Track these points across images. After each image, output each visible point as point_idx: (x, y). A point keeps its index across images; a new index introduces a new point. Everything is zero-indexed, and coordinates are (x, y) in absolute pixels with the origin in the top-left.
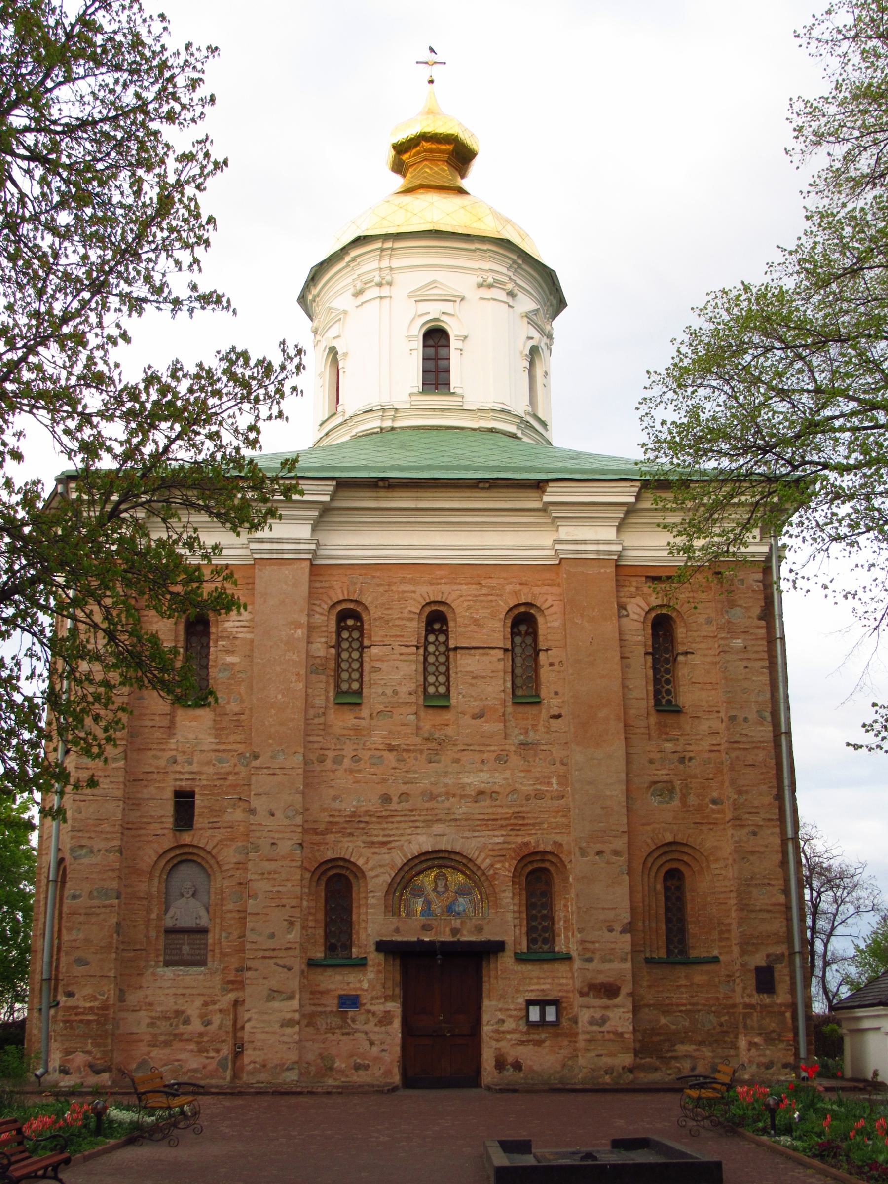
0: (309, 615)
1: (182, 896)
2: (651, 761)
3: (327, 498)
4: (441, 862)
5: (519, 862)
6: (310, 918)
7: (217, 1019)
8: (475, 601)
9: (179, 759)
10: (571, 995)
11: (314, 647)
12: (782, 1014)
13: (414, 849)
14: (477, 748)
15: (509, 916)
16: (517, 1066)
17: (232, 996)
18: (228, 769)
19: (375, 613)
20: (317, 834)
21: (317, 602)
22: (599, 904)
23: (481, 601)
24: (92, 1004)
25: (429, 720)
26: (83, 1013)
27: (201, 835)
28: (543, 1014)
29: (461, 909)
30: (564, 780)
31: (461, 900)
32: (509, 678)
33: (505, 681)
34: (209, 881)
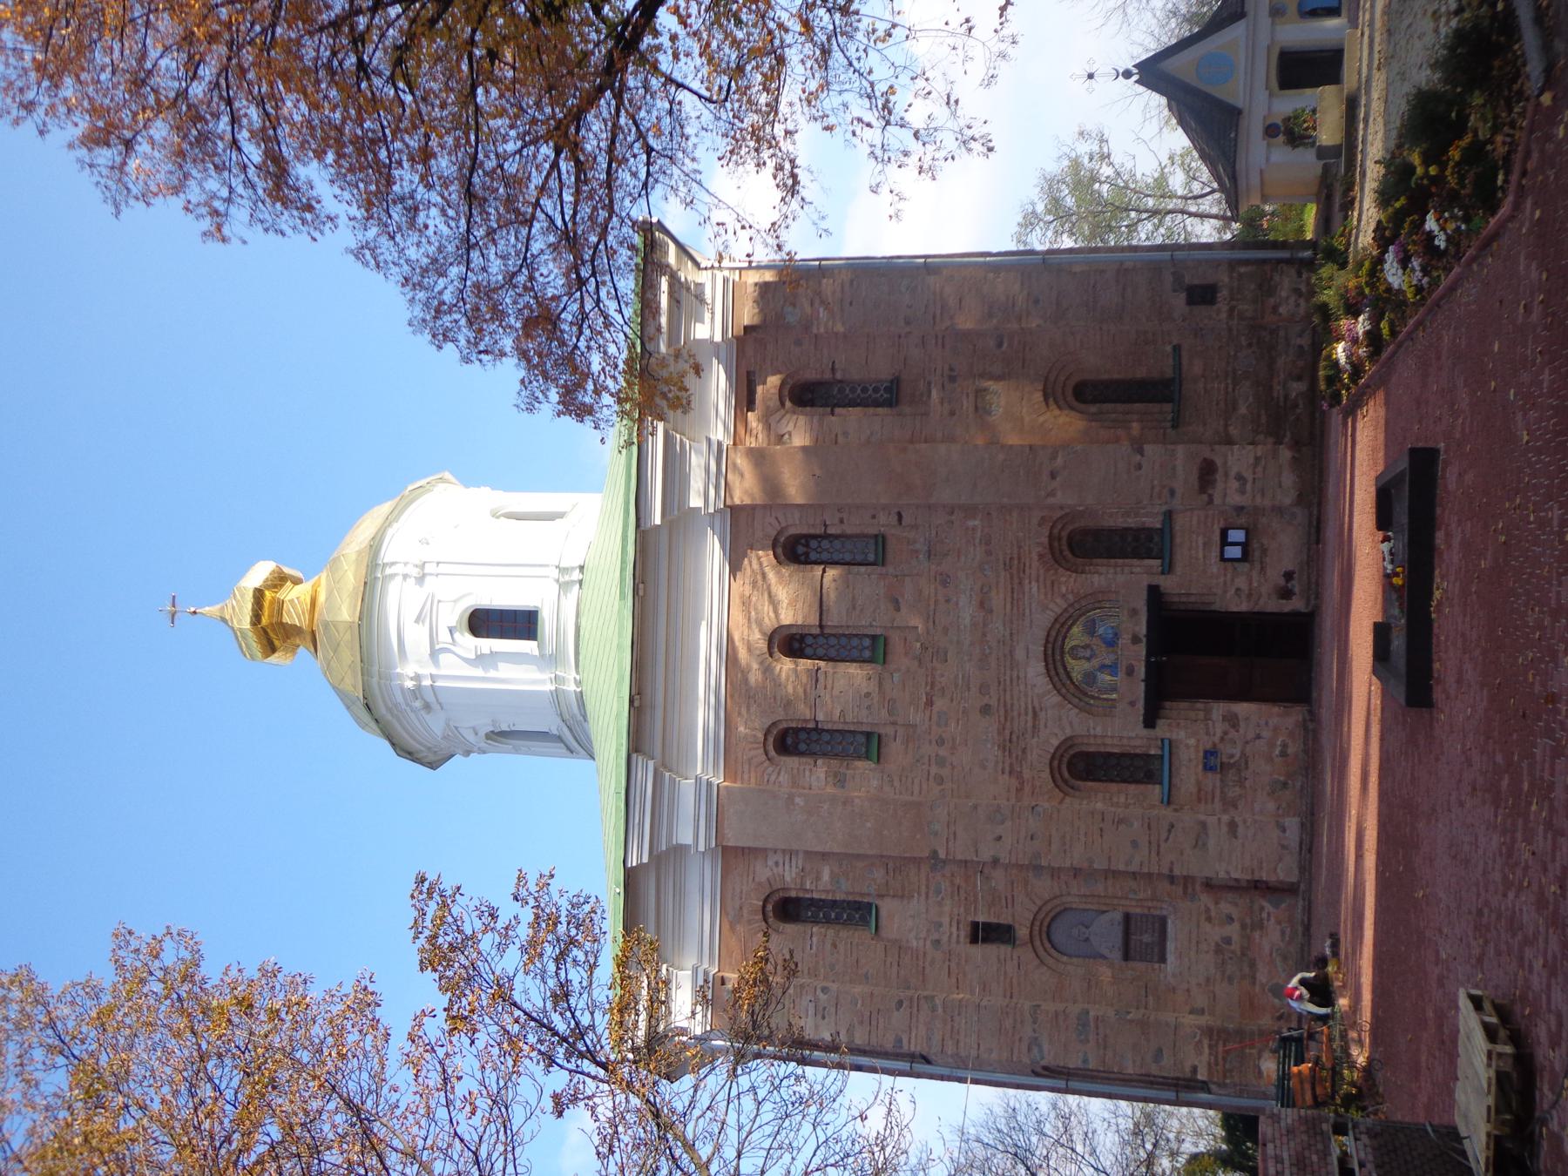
1: (1087, 940)
2: (952, 413)
3: (651, 764)
4: (1058, 652)
9: (936, 936)
12: (1241, 275)
15: (1121, 578)
16: (1289, 576)
19: (780, 714)
25: (900, 660)
27: (1020, 917)
30: (970, 511)
31: (1101, 631)
32: (856, 569)
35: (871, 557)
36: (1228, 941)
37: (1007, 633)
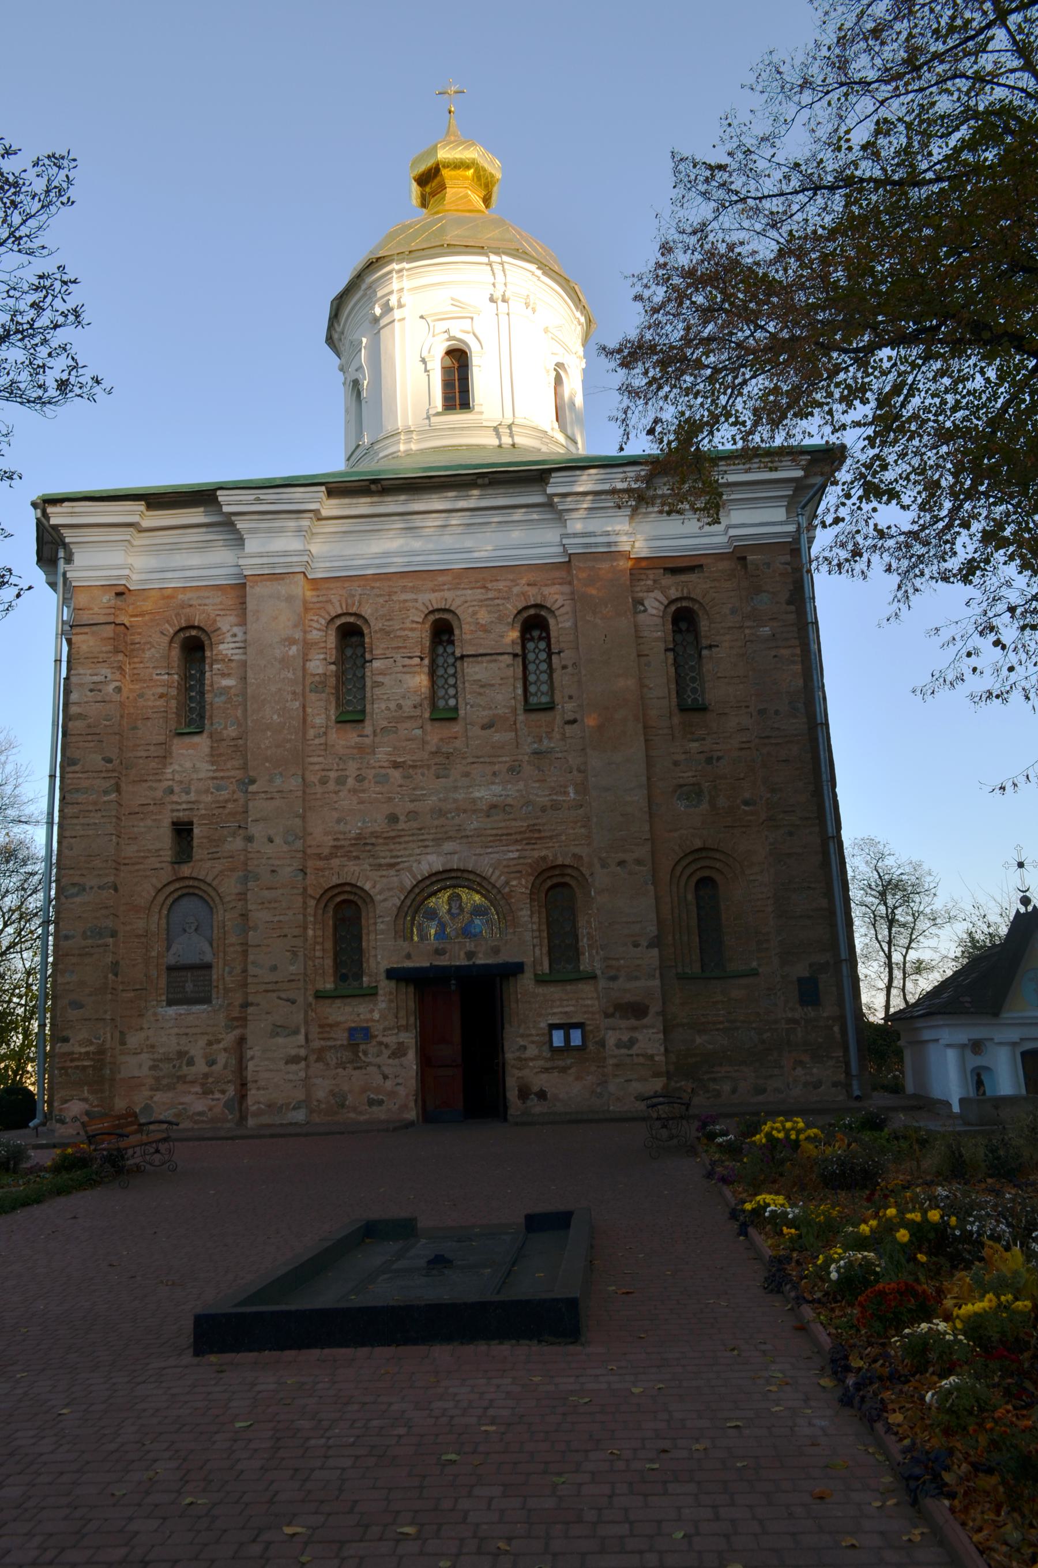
2: (676, 763)
5: (537, 877)
6: (318, 947)
7: (222, 1059)
9: (177, 789)
10: (597, 1016)
14: (487, 760)
15: (528, 936)
16: (542, 1095)
17: (237, 1032)
18: (227, 796)
19: (376, 625)
20: (321, 859)
21: (315, 618)
23: (487, 606)
24: (88, 1049)
25: (435, 735)
26: (78, 1059)
27: (202, 866)
28: (567, 1038)
30: (582, 788)
31: (477, 922)
32: (519, 685)
33: (515, 688)
35: (533, 700)
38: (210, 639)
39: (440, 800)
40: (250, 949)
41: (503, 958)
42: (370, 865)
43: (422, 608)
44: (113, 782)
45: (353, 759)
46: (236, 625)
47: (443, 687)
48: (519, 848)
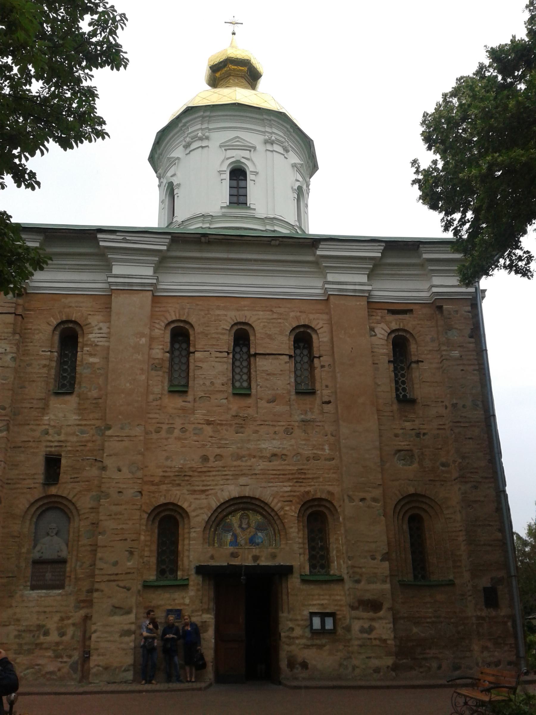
0: (152, 329)
1: (48, 534)
2: (396, 436)
3: (165, 248)
5: (302, 506)
6: (147, 549)
7: (70, 631)
8: (269, 323)
9: (51, 431)
10: (344, 608)
11: (154, 352)
13: (225, 496)
14: (271, 423)
15: (296, 547)
16: (304, 665)
17: (82, 612)
20: (153, 485)
21: (156, 321)
22: (364, 538)
23: (273, 323)
25: (235, 405)
27: (65, 488)
28: (323, 623)
29: (260, 541)
31: (259, 534)
32: (293, 375)
33: (290, 377)
34: (70, 522)
36: (46, 633)
37: (257, 472)
38: (83, 330)
39: (238, 448)
40: (99, 550)
41: (280, 561)
42: (188, 491)
43: (229, 320)
44: (5, 423)
45: (179, 416)
46: (102, 322)
47: (239, 374)
48: (291, 484)
